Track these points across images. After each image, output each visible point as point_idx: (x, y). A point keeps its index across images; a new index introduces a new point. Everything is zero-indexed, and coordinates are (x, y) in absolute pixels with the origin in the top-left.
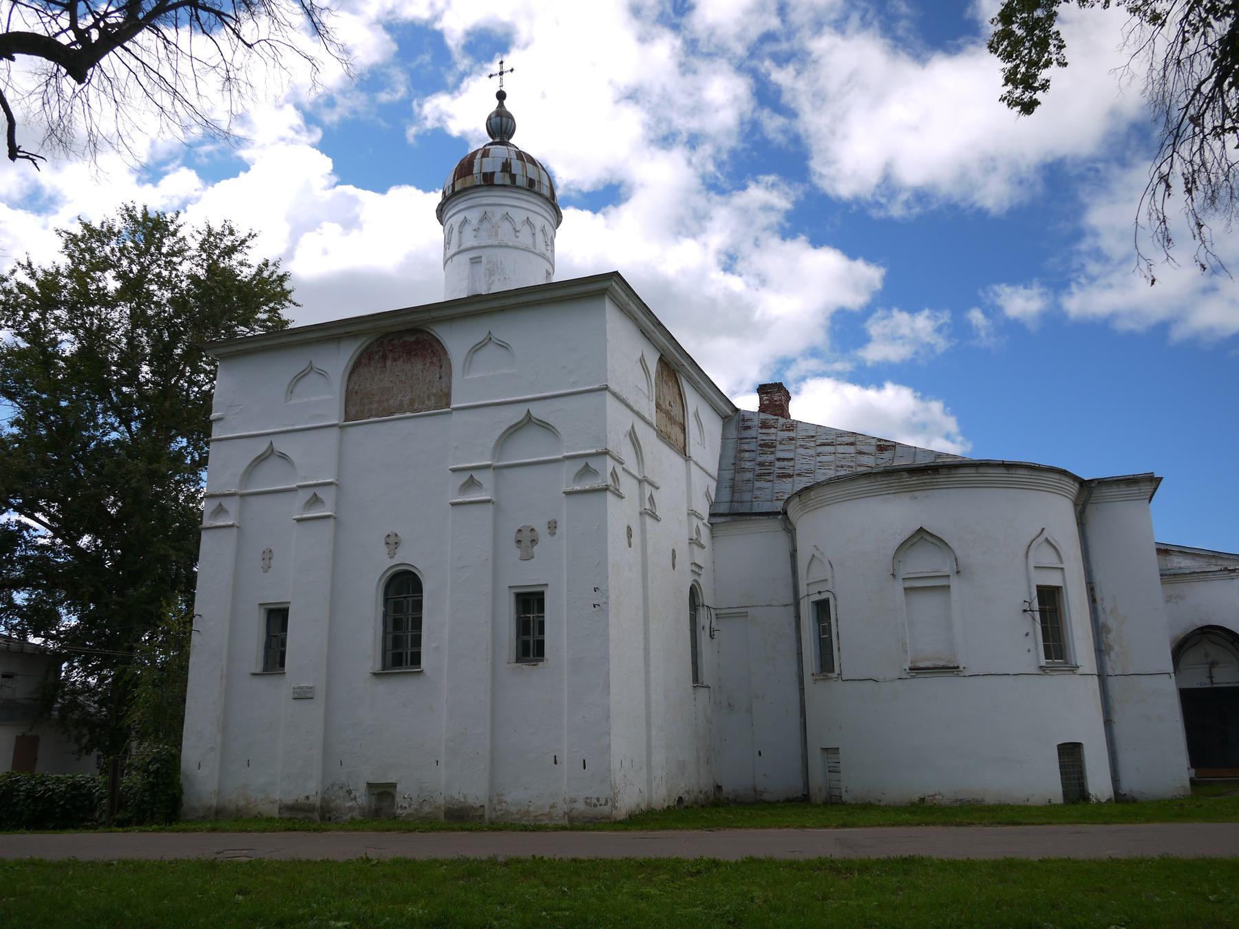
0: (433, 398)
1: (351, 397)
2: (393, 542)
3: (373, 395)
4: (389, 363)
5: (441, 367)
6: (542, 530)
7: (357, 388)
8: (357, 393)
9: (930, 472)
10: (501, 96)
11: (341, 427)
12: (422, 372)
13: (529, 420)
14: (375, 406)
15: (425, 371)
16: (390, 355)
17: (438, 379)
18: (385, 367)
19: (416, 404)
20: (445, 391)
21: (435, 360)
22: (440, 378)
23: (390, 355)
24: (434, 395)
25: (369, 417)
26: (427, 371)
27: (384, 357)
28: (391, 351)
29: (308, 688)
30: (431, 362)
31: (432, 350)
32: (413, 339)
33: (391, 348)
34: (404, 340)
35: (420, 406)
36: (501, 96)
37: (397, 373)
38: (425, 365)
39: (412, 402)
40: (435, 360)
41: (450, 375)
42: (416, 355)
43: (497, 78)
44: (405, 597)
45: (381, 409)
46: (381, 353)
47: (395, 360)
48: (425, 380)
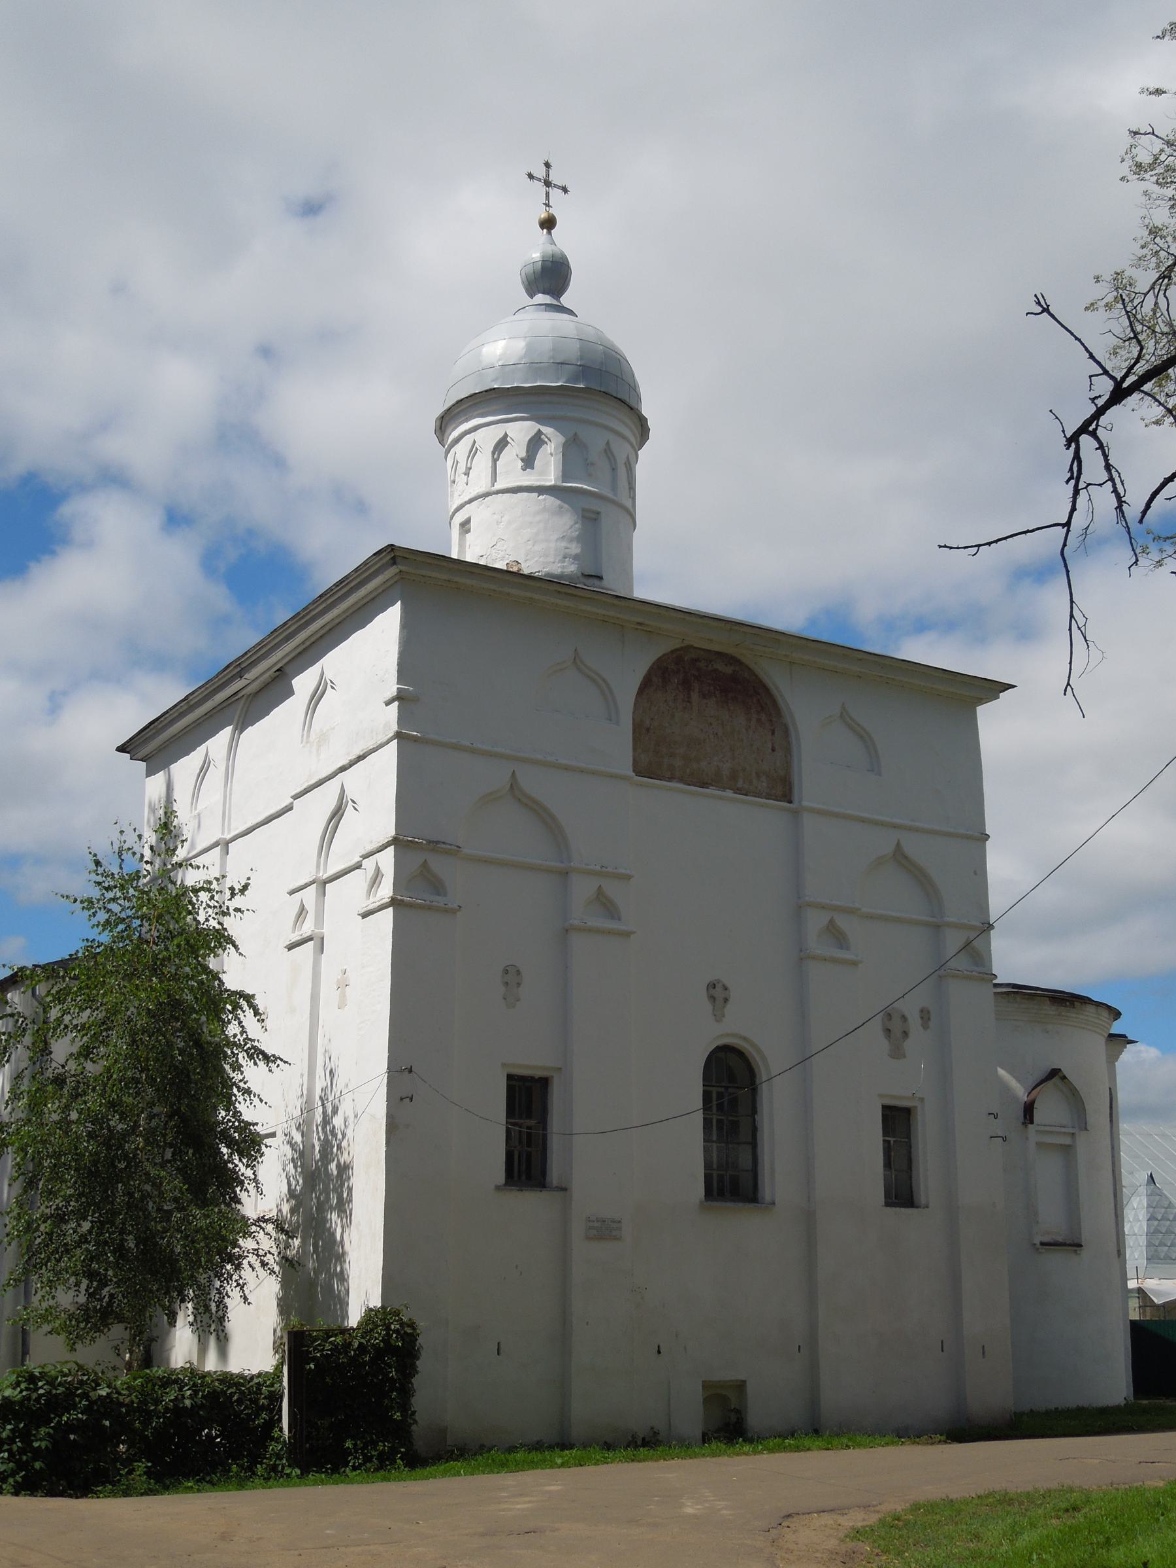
1: (639, 730)
2: (718, 994)
4: (695, 697)
5: (773, 733)
6: (915, 1022)
8: (648, 730)
9: (1068, 1003)
10: (548, 224)
12: (747, 730)
13: (900, 857)
17: (770, 751)
18: (689, 702)
21: (763, 717)
22: (773, 750)
25: (670, 779)
26: (754, 732)
29: (613, 1221)
30: (759, 720)
31: (758, 700)
33: (696, 673)
36: (548, 224)
39: (734, 776)
41: (788, 750)
44: (727, 1087)
45: (688, 770)
47: (704, 696)
48: (752, 745)
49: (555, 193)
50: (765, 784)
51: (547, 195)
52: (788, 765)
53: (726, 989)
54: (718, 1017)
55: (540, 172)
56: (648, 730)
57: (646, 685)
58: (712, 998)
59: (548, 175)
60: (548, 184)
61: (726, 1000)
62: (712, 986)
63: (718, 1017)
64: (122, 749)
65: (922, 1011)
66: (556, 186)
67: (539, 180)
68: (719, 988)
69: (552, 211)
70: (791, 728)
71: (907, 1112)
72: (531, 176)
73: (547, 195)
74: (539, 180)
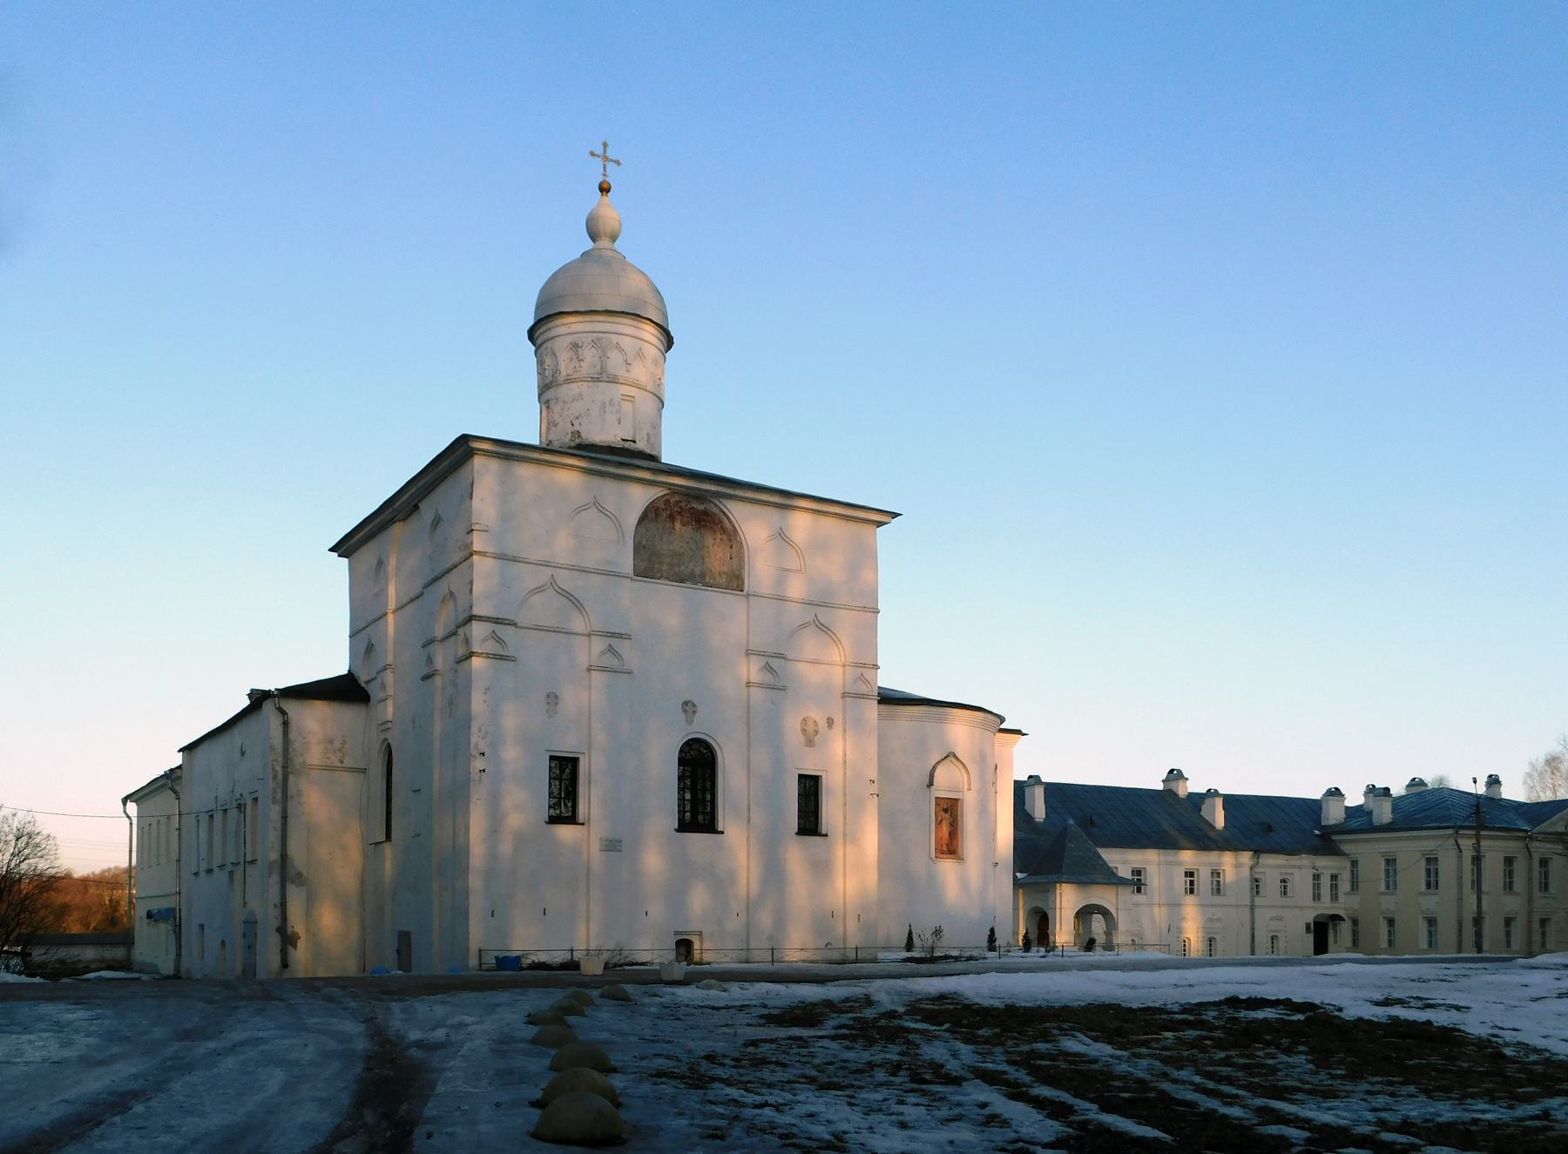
0: (724, 576)
1: (638, 549)
2: (689, 707)
3: (663, 555)
4: (678, 525)
7: (644, 542)
10: (604, 189)
11: (631, 578)
14: (665, 567)
15: (715, 546)
16: (678, 518)
19: (708, 578)
20: (737, 572)
23: (678, 518)
24: (725, 573)
27: (672, 518)
28: (680, 513)
32: (701, 507)
34: (692, 506)
35: (711, 581)
36: (604, 189)
37: (687, 540)
38: (715, 539)
40: (724, 537)
42: (705, 526)
43: (599, 162)
46: (668, 512)
49: (610, 166)
50: (724, 580)
51: (605, 168)
52: (741, 567)
53: (695, 706)
54: (690, 722)
55: (599, 151)
56: (644, 547)
57: (643, 518)
58: (685, 711)
59: (605, 152)
60: (606, 159)
61: (694, 712)
62: (686, 703)
63: (690, 722)
64: (330, 550)
65: (828, 719)
66: (611, 160)
67: (599, 156)
68: (689, 705)
69: (607, 180)
70: (744, 544)
71: (815, 780)
72: (592, 154)
73: (605, 168)
74: (599, 156)
